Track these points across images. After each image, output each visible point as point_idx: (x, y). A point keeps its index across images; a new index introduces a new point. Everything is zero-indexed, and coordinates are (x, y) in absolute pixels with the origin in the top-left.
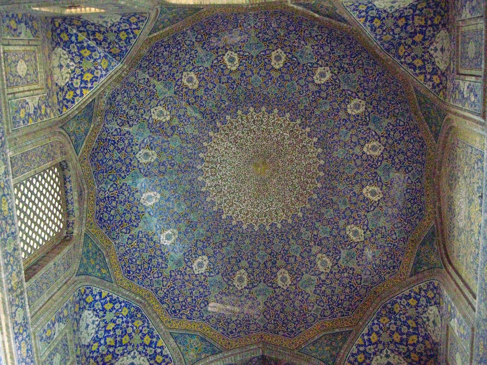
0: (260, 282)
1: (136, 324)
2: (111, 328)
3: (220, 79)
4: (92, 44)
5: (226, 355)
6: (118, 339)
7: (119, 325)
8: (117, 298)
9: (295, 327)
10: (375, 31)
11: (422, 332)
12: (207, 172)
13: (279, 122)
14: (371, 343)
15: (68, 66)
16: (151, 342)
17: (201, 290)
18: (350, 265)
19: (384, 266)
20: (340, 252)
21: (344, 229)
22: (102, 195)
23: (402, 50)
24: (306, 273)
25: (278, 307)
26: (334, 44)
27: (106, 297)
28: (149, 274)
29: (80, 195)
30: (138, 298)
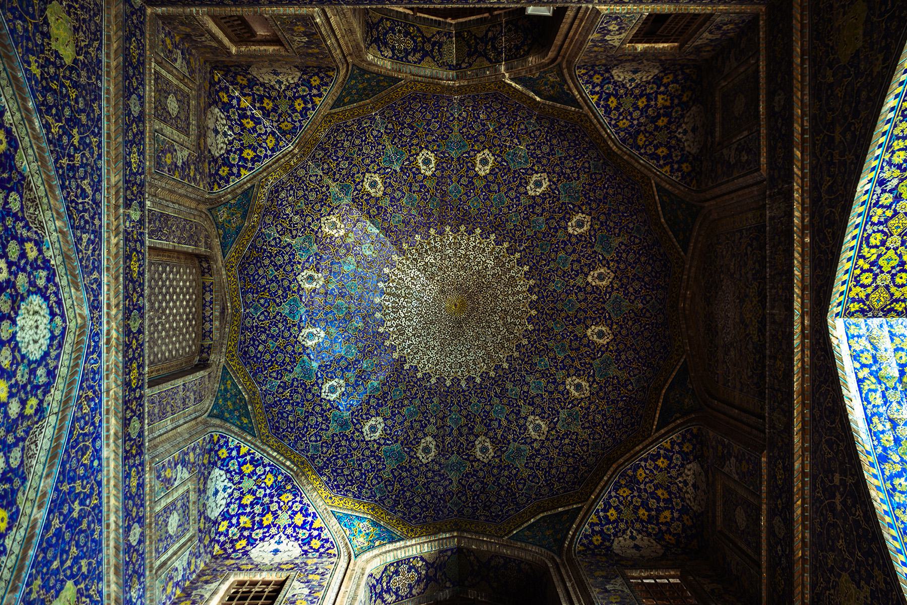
1: (283, 498)
2: (248, 503)
3: (411, 186)
4: (258, 114)
5: (408, 543)
6: (257, 519)
7: (260, 498)
8: (261, 458)
10: (610, 113)
13: (482, 246)
14: (609, 522)
15: (225, 134)
16: (305, 523)
18: (573, 429)
19: (618, 426)
20: (558, 413)
21: (564, 383)
22: (248, 322)
24: (514, 441)
26: (554, 142)
28: (304, 436)
30: (288, 463)
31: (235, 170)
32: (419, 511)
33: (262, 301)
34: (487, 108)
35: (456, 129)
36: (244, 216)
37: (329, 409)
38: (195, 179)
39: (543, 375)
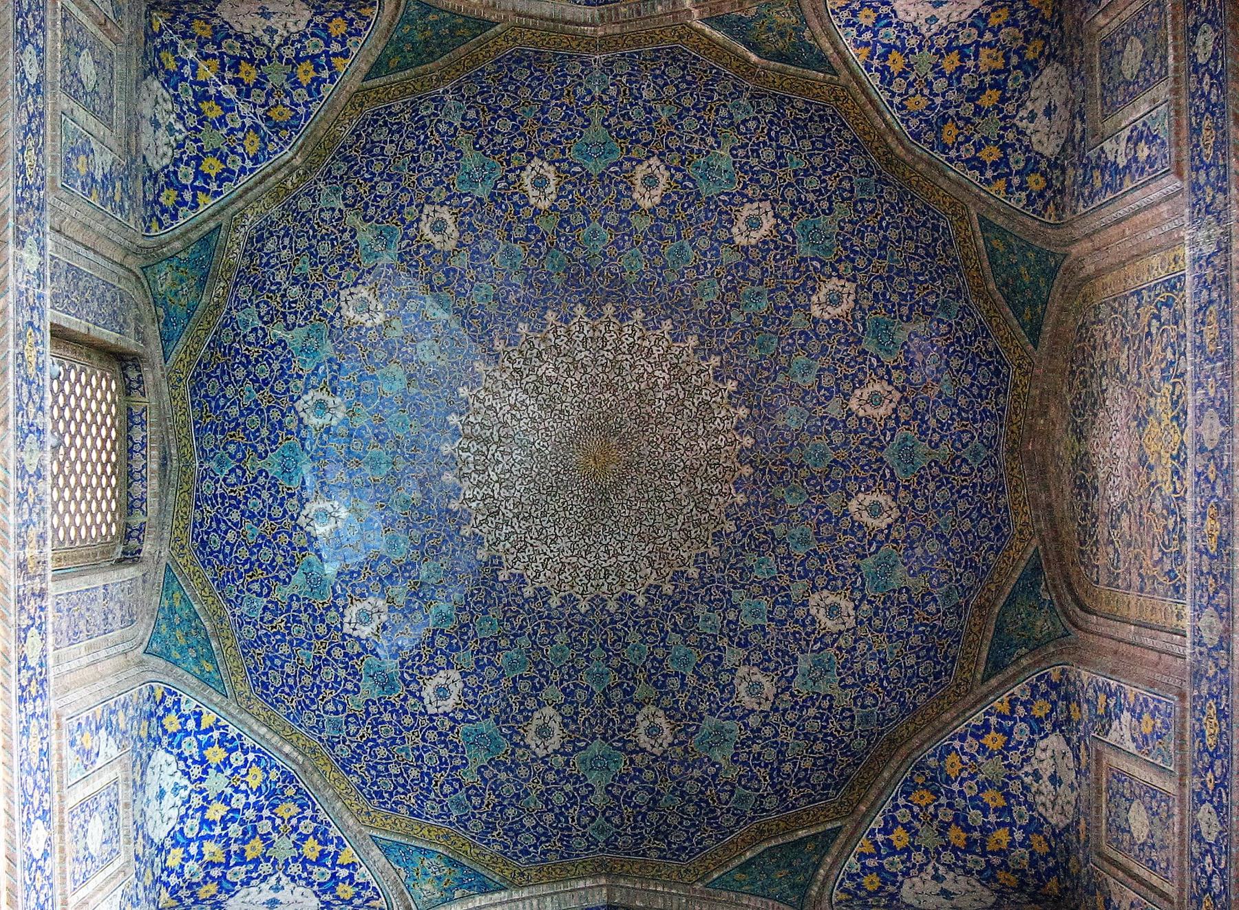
0: (594, 738)
4: (229, 92)
5: (516, 896)
8: (239, 736)
9: (689, 839)
11: (1021, 817)
12: (465, 462)
13: (646, 343)
14: (893, 851)
15: (170, 129)
16: (323, 854)
17: (444, 753)
18: (823, 688)
20: (795, 660)
22: (207, 488)
23: (949, 133)
24: (712, 713)
25: (642, 798)
27: (211, 729)
28: (313, 701)
29: (164, 461)
31: (188, 196)
32: (533, 841)
33: (232, 448)
34: (656, 77)
35: (596, 120)
36: (202, 284)
37: (359, 655)
38: (122, 208)
39: (766, 588)
